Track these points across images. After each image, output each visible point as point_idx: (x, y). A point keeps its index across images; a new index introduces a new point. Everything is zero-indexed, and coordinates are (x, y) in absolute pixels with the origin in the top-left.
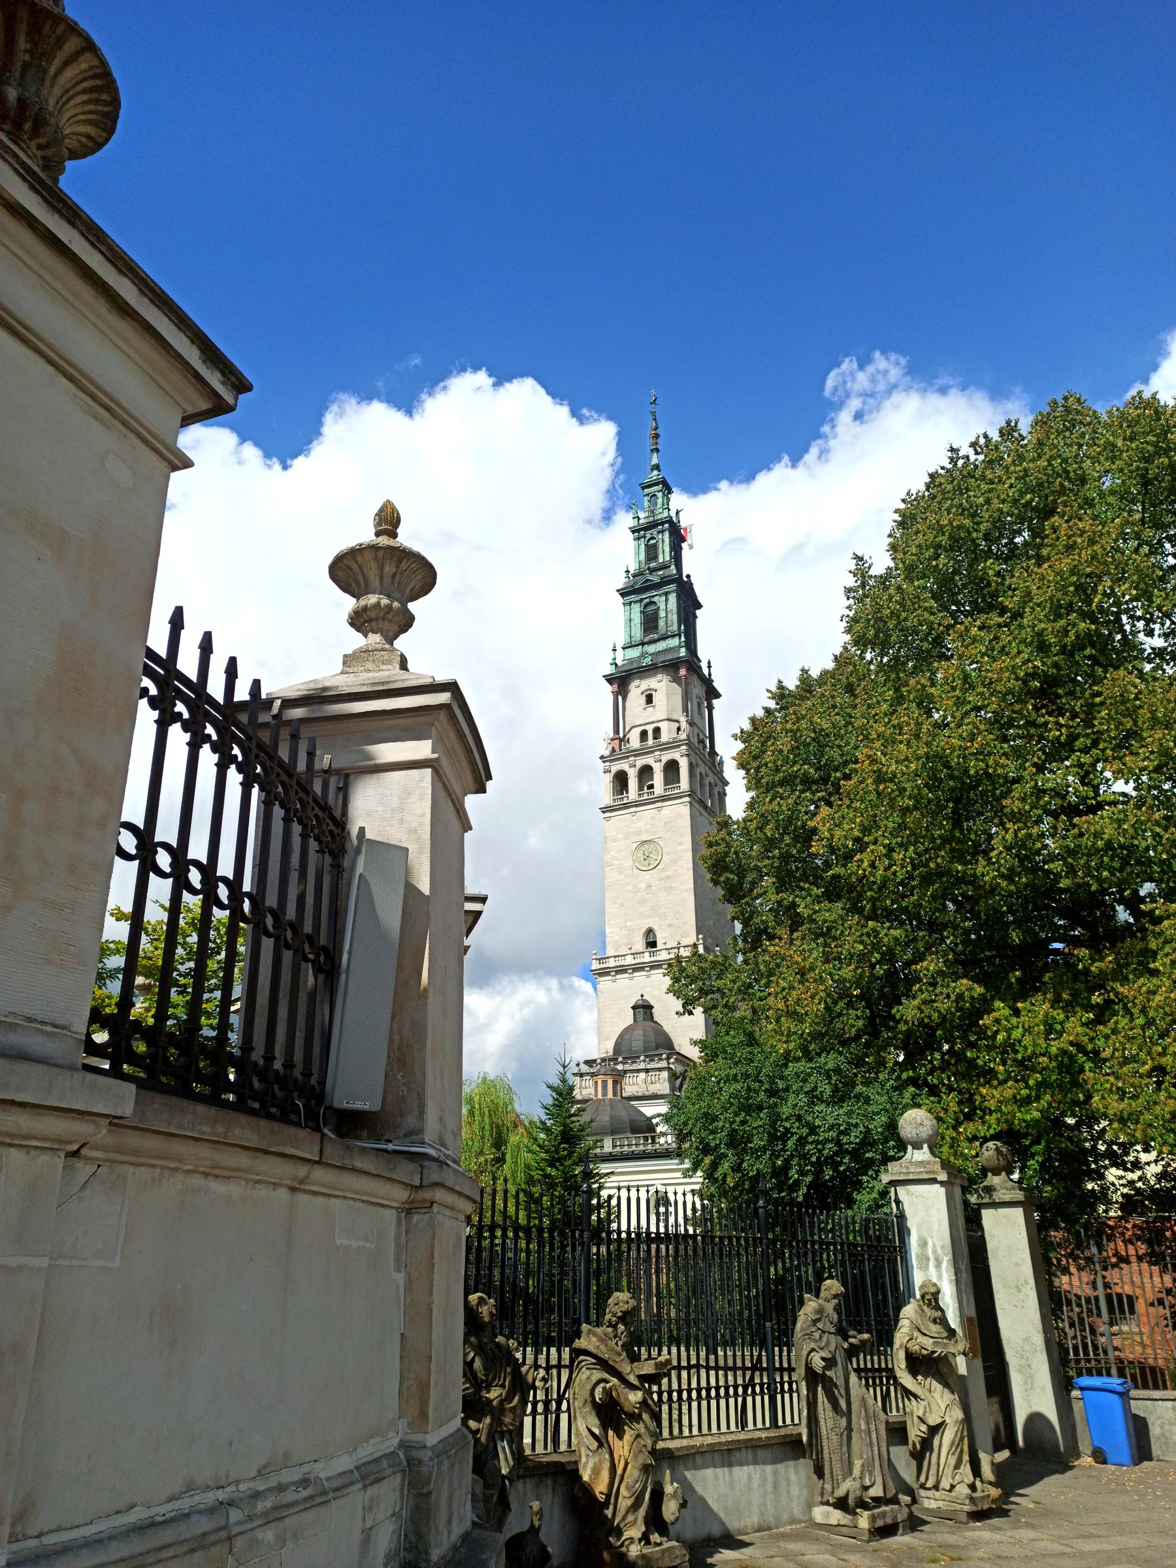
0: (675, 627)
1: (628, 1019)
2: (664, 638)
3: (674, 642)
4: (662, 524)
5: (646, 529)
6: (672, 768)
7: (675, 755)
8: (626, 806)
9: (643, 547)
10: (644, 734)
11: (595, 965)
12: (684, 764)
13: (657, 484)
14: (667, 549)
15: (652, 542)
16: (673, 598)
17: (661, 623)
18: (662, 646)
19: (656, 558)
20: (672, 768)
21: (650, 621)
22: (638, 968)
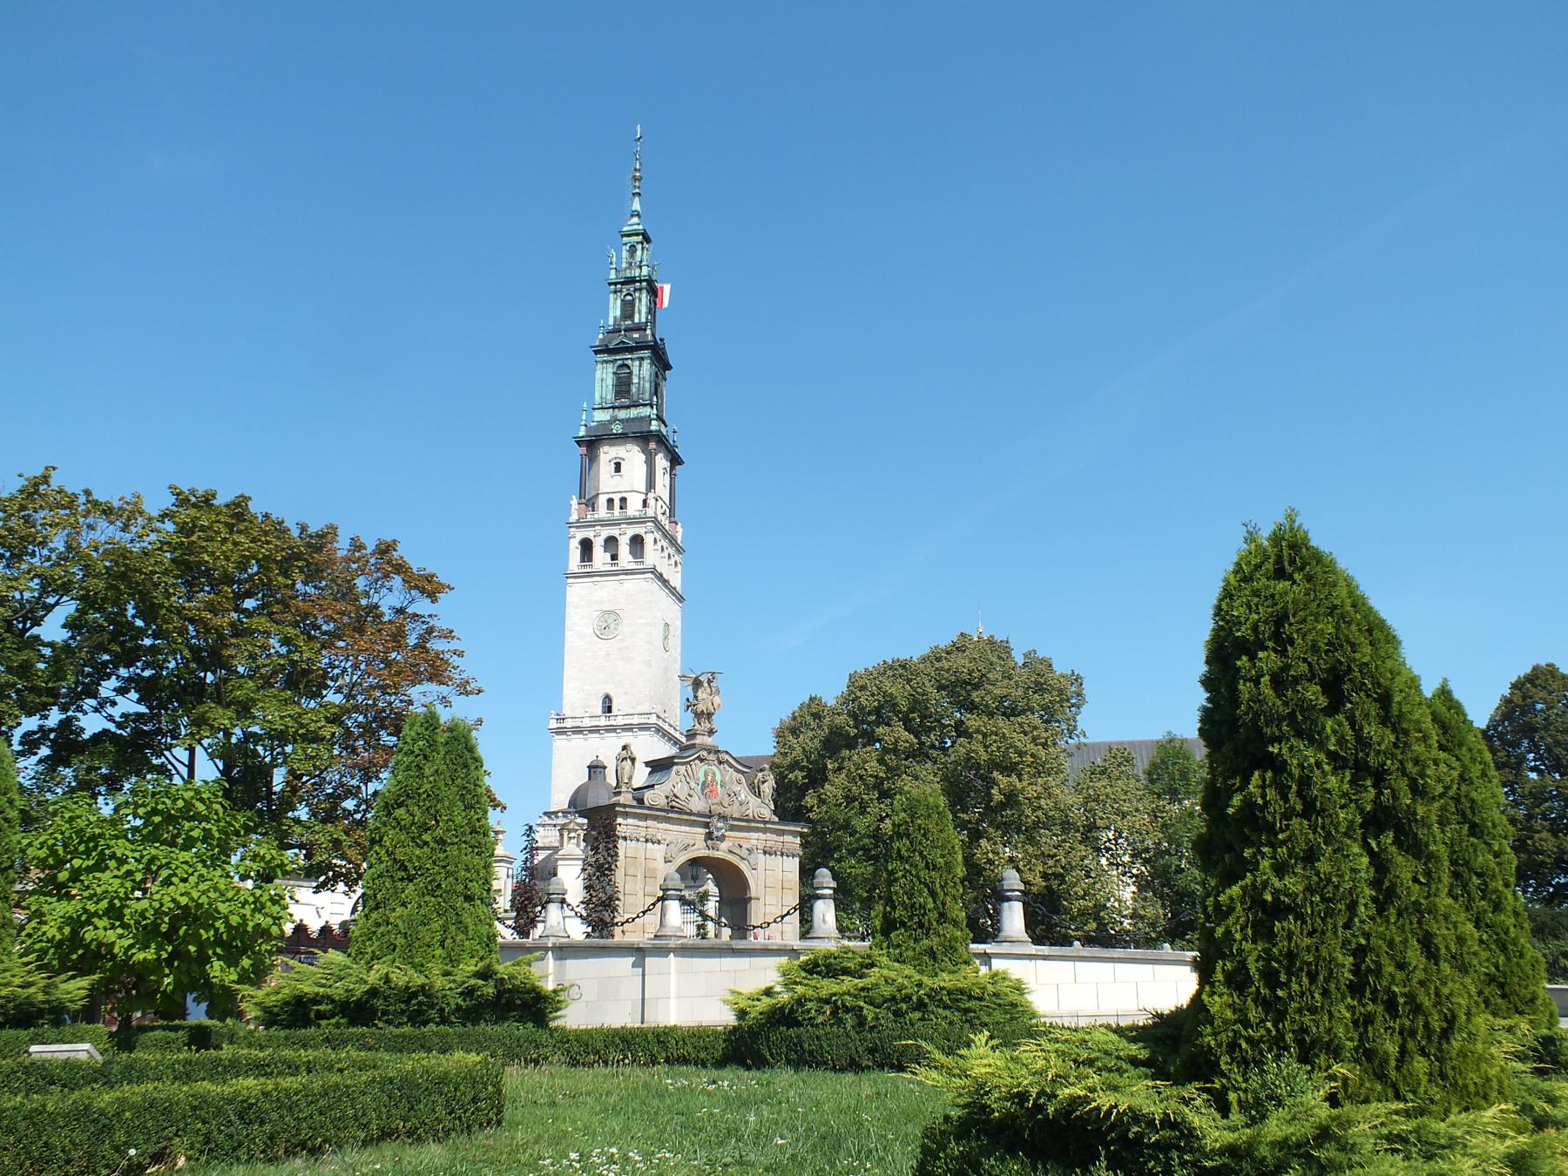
0: (647, 396)
3: (646, 411)
5: (622, 283)
6: (637, 541)
7: (639, 530)
10: (610, 501)
11: (553, 724)
12: (649, 540)
14: (644, 310)
16: (646, 364)
17: (634, 390)
18: (633, 413)
19: (631, 317)
20: (637, 541)
21: (622, 385)
22: (595, 730)
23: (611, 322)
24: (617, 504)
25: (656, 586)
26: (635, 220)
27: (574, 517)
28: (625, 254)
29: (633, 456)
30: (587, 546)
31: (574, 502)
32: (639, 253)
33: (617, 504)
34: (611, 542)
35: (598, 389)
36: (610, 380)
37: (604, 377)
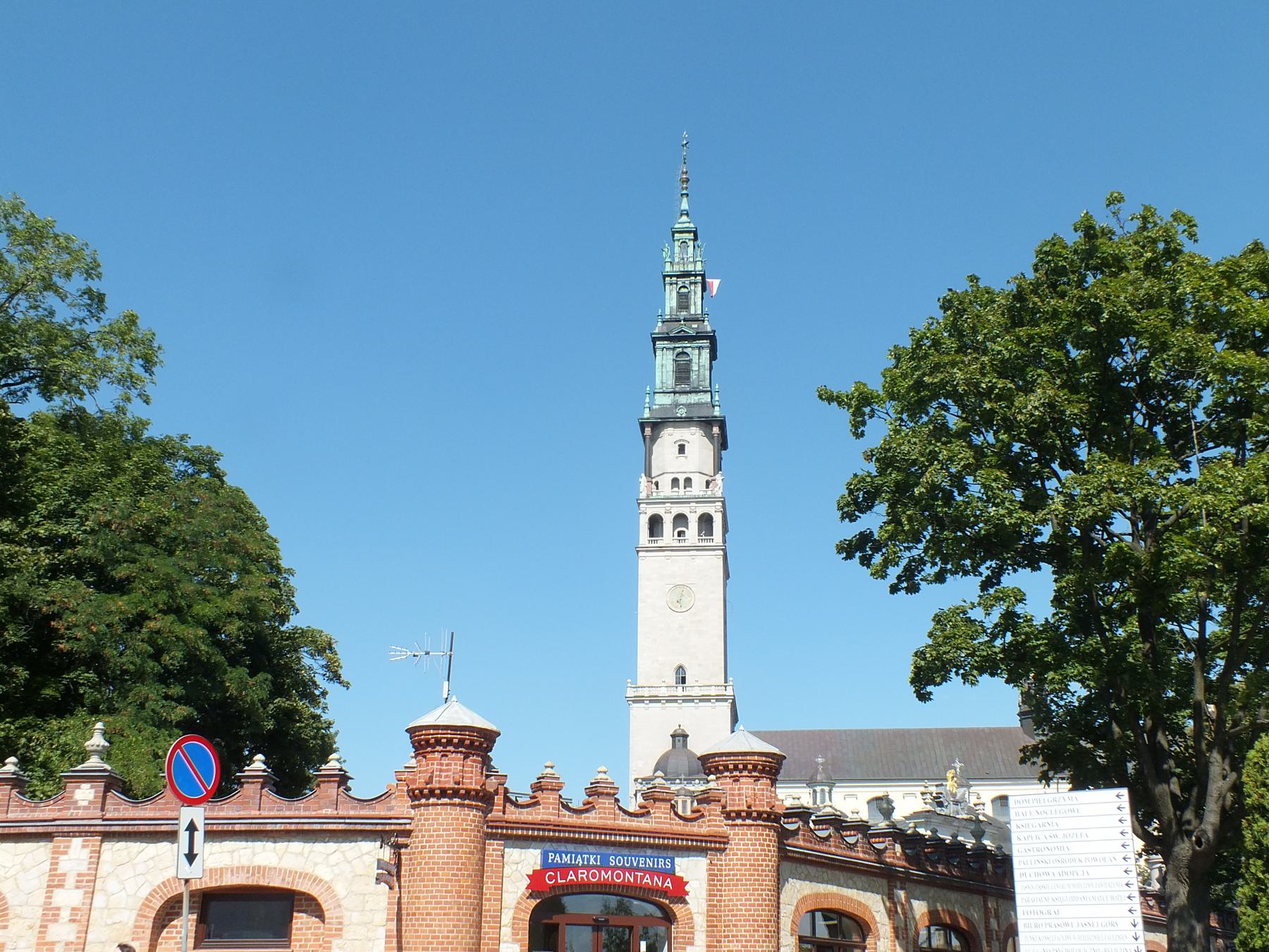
1: (667, 745)
2: (696, 391)
4: (696, 275)
6: (706, 521)
8: (661, 549)
9: (674, 294)
10: (675, 482)
11: (630, 693)
13: (689, 232)
15: (683, 290)
16: (706, 354)
17: (694, 376)
18: (693, 398)
19: (687, 308)
20: (706, 521)
21: (682, 372)
22: (672, 700)
23: (667, 311)
24: (682, 483)
26: (684, 218)
27: (643, 495)
30: (655, 524)
33: (682, 483)
35: (658, 374)
36: (670, 366)
37: (665, 362)
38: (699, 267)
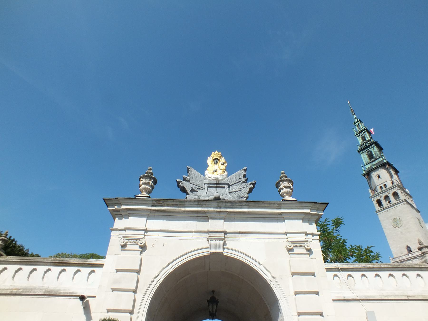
0: (379, 155)
2: (377, 159)
3: (381, 159)
4: (364, 130)
6: (395, 194)
8: (384, 209)
9: (360, 138)
10: (381, 187)
12: (399, 192)
14: (368, 136)
16: (375, 148)
17: (374, 155)
18: (377, 161)
19: (365, 139)
20: (395, 194)
21: (371, 156)
23: (360, 143)
25: (408, 206)
27: (371, 195)
28: (357, 128)
29: (383, 172)
30: (379, 203)
31: (370, 191)
32: (361, 125)
34: (387, 198)
37: (364, 157)
38: (364, 127)
